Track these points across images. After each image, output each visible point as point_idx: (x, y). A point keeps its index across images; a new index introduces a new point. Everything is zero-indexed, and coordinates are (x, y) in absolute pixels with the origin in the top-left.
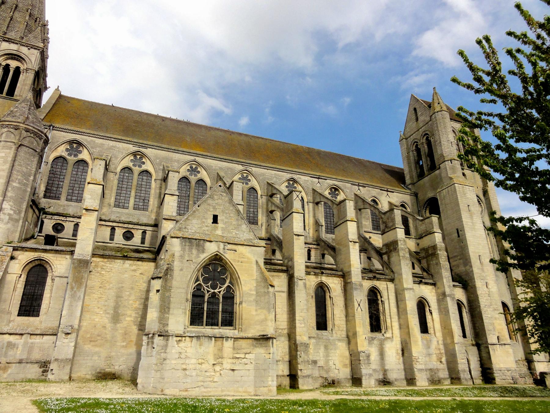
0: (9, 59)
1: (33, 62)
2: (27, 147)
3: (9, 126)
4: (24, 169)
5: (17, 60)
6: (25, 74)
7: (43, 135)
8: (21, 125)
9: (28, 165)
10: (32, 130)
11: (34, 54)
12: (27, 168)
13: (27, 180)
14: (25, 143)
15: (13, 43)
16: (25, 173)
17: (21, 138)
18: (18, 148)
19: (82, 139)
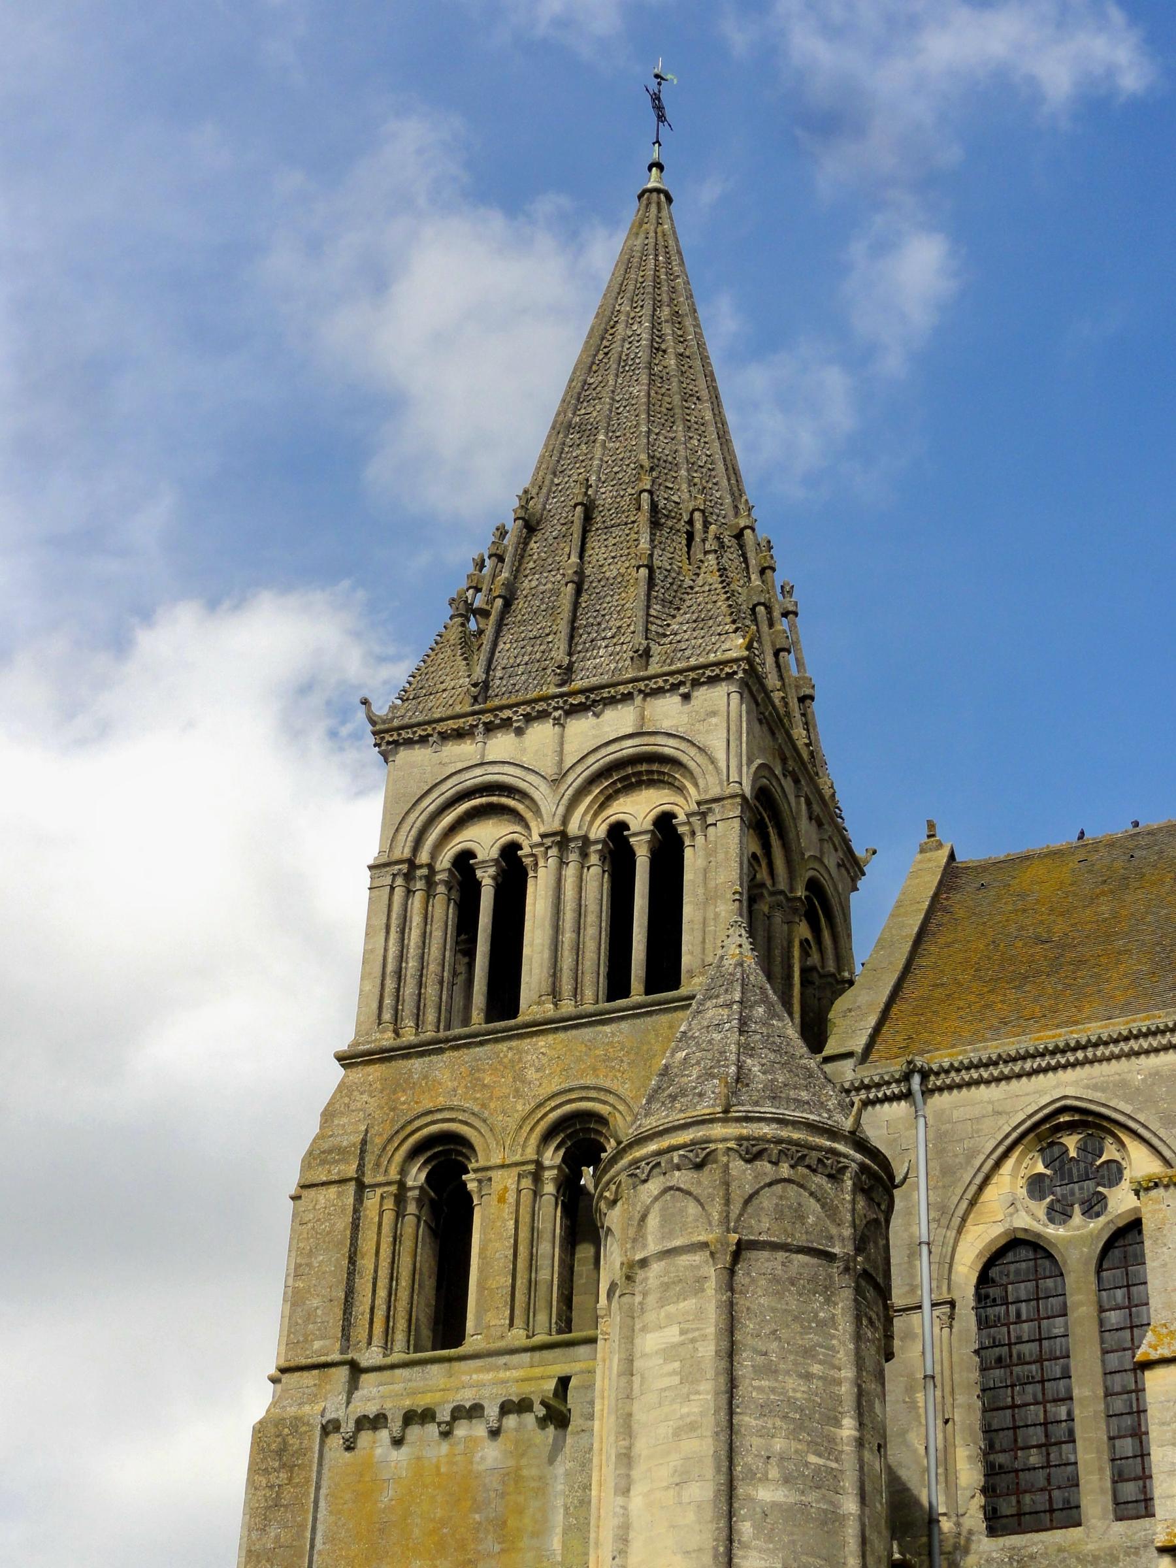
0: (617, 792)
1: (721, 756)
2: (774, 1247)
3: (663, 1160)
4: (794, 1387)
5: (651, 783)
6: (700, 839)
7: (841, 1147)
8: (718, 1130)
9: (808, 1353)
10: (779, 1141)
11: (714, 714)
12: (808, 1377)
13: (828, 1446)
14: (762, 1226)
15: (612, 701)
16: (801, 1410)
17: (735, 1209)
18: (732, 1272)
19: (1095, 1088)
